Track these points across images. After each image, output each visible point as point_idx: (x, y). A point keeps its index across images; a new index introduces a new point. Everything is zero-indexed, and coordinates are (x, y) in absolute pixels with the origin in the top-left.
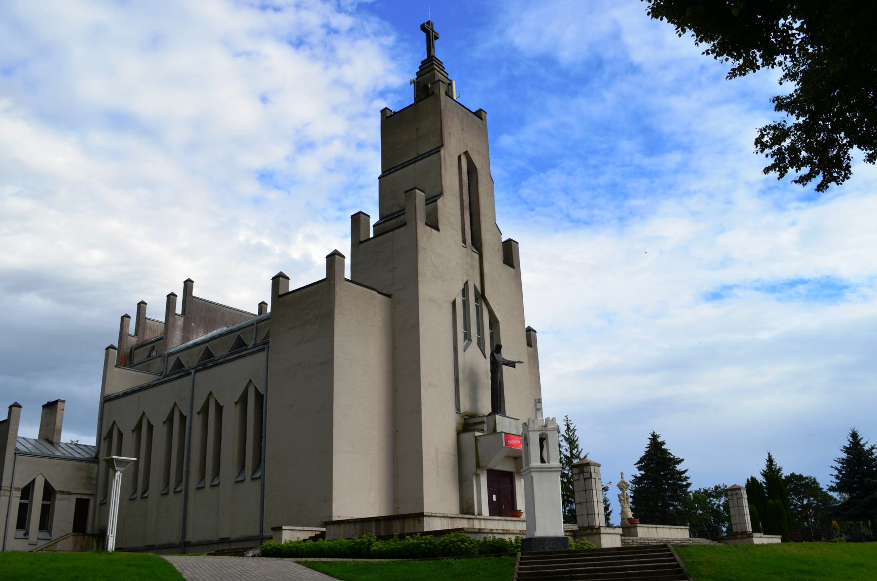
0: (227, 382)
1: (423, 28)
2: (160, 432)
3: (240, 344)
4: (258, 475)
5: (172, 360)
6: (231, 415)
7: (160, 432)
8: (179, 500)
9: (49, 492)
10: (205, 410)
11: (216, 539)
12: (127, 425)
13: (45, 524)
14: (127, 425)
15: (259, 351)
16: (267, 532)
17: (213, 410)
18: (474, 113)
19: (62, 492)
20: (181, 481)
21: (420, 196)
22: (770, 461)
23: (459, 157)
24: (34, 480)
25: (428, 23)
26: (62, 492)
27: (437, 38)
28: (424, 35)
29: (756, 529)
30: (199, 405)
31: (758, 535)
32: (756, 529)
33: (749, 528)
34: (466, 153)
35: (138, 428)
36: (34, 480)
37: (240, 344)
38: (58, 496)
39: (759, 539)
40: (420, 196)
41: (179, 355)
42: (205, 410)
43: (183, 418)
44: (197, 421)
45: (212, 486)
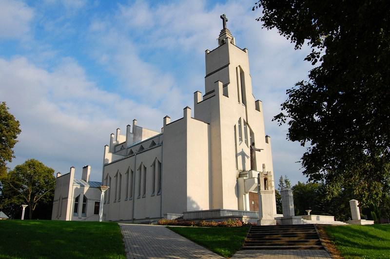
0: (148, 158)
1: (221, 17)
2: (124, 177)
3: (154, 143)
4: (159, 194)
5: (129, 150)
6: (150, 171)
7: (124, 177)
8: (131, 201)
9: (85, 200)
10: (140, 168)
11: (144, 218)
12: (112, 175)
13: (84, 211)
14: (112, 175)
15: (159, 146)
16: (162, 216)
17: (143, 168)
18: (243, 50)
19: (90, 199)
20: (132, 196)
21: (221, 84)
22: (242, 149)
23: (237, 68)
24: (80, 195)
25: (223, 15)
26: (90, 199)
27: (227, 21)
28: (222, 20)
29: (362, 218)
30: (138, 167)
31: (363, 220)
32: (362, 218)
33: (359, 218)
34: (239, 66)
35: (117, 175)
36: (80, 195)
37: (154, 143)
38: (88, 201)
39: (364, 222)
40: (221, 84)
41: (132, 149)
42: (140, 168)
43: (132, 172)
44: (137, 173)
45: (143, 198)
